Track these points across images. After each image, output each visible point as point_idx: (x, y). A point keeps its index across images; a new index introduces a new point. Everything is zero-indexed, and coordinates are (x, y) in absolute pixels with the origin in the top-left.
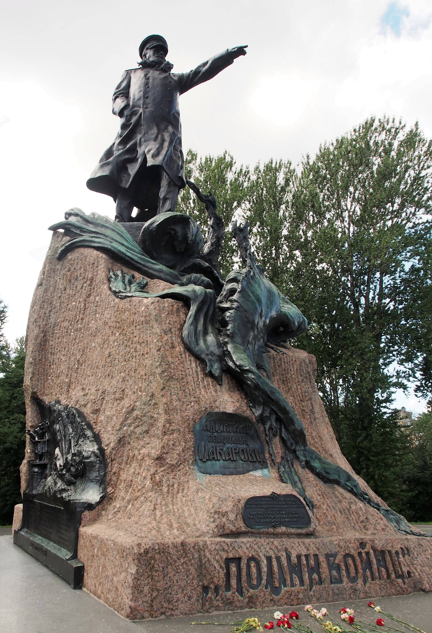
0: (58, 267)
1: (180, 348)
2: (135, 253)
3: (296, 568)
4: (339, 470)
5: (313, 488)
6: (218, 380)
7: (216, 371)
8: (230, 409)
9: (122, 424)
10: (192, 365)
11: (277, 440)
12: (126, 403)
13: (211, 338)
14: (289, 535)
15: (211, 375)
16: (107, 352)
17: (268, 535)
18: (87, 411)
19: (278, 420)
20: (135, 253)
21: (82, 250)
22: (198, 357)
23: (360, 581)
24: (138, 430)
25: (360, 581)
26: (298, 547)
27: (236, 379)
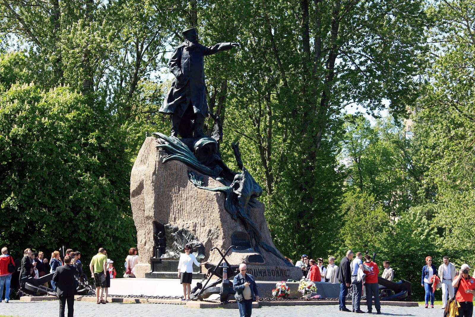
0: (163, 166)
1: (225, 211)
2: (196, 163)
3: (260, 272)
4: (271, 247)
5: (265, 254)
6: (236, 221)
7: (236, 218)
8: (241, 230)
9: (208, 235)
10: (229, 217)
11: (254, 239)
12: (207, 228)
13: (233, 206)
14: (258, 265)
15: (234, 219)
16: (194, 208)
17: (254, 265)
18: (191, 229)
19: (254, 233)
20: (196, 163)
21: (175, 161)
22: (229, 213)
23: (275, 276)
24: (214, 237)
25: (275, 276)
26: (261, 268)
27: (243, 222)
